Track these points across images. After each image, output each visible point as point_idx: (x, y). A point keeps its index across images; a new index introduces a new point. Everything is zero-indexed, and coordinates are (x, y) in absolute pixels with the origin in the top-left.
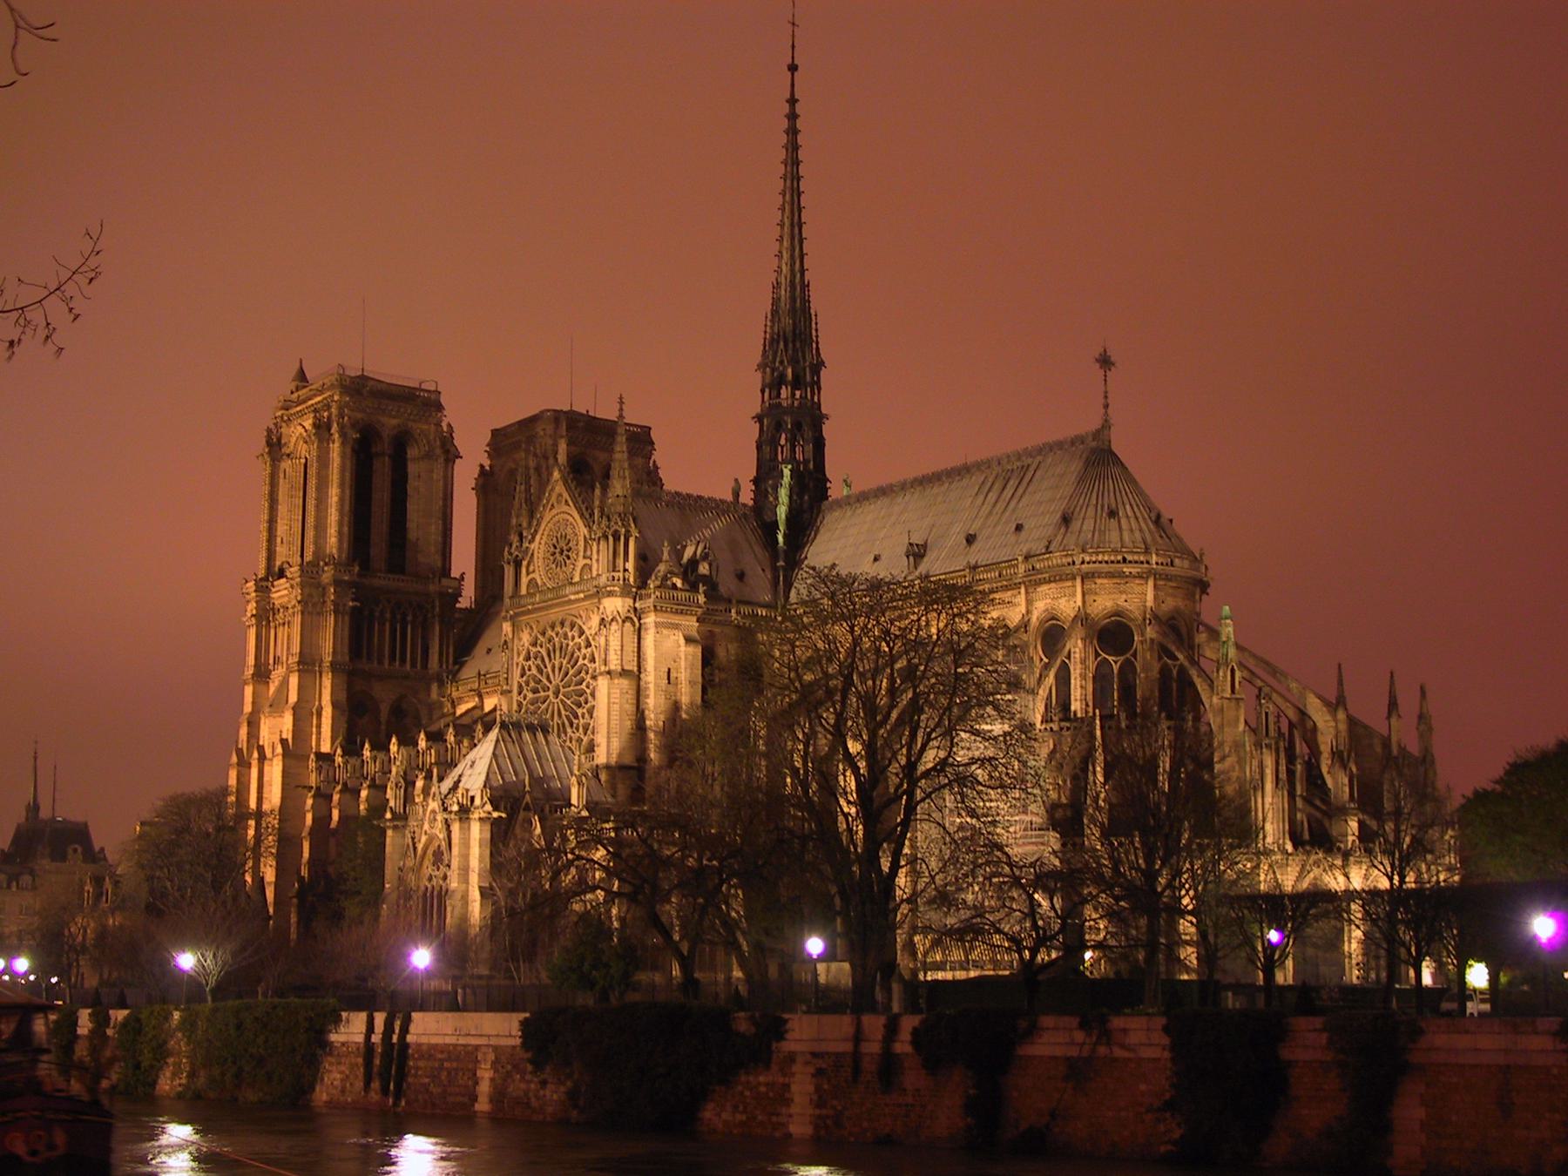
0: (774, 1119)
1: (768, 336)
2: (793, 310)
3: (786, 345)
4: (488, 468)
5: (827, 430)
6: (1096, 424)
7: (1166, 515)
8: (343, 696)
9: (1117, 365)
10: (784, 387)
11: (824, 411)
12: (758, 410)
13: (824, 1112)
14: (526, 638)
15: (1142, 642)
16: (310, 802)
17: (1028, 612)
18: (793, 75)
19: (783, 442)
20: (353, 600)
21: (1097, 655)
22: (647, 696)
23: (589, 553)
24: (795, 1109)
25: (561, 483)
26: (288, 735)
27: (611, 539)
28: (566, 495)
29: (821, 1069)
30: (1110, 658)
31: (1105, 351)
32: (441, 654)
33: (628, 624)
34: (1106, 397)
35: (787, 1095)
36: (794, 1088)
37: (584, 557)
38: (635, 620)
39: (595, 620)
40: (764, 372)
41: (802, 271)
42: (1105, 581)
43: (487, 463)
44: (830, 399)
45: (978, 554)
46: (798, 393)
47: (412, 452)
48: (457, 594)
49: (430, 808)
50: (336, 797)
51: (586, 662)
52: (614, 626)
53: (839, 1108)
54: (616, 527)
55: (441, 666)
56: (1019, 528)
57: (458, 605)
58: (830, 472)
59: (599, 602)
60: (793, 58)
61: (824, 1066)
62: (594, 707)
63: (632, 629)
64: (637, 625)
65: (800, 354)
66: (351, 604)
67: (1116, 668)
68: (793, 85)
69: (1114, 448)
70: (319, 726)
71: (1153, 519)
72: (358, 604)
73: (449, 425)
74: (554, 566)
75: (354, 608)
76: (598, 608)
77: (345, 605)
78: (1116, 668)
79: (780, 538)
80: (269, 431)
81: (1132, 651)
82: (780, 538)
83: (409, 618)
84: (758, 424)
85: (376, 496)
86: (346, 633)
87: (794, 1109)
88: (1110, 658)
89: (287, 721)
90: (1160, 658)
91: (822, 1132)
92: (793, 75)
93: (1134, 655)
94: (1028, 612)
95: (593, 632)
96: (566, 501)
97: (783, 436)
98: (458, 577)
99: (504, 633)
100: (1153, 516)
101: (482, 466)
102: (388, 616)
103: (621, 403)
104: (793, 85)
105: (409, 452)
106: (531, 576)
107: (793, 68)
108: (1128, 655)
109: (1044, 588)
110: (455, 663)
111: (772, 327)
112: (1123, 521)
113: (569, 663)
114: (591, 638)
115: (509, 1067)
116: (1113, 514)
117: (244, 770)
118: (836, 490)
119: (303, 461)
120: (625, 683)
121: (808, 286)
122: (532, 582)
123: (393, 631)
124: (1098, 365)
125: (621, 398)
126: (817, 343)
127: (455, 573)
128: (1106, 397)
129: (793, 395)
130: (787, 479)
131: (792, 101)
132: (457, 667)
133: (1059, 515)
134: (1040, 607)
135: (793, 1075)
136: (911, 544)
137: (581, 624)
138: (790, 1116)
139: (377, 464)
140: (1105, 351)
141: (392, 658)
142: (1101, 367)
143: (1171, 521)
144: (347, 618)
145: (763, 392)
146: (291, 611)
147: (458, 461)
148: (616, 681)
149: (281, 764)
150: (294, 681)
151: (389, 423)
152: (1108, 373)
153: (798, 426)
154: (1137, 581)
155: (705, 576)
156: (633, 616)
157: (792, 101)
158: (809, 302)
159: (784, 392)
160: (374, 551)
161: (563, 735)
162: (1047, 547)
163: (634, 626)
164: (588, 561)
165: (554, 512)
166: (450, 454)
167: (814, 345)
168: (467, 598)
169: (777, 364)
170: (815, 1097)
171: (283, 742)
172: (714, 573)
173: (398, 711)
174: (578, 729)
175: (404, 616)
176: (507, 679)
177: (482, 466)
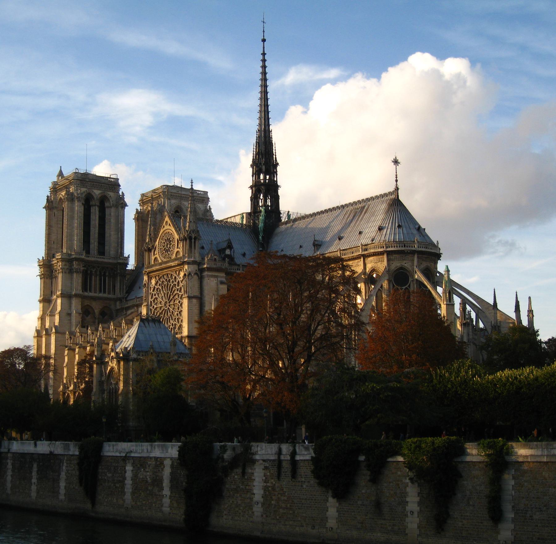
0: (247, 487)
1: (255, 153)
2: (265, 142)
3: (262, 157)
4: (139, 210)
5: (280, 192)
6: (392, 189)
7: (423, 226)
8: (80, 307)
9: (401, 163)
10: (262, 174)
11: (279, 184)
13: (268, 484)
14: (153, 282)
15: (413, 281)
16: (66, 352)
18: (264, 43)
19: (261, 197)
20: (83, 267)
21: (394, 286)
22: (205, 306)
23: (179, 246)
24: (255, 483)
25: (167, 217)
26: (57, 323)
27: (188, 241)
28: (169, 222)
29: (266, 466)
31: (396, 157)
32: (120, 289)
33: (196, 277)
34: (396, 177)
35: (253, 478)
36: (255, 474)
37: (177, 248)
38: (199, 274)
39: (182, 274)
40: (253, 168)
41: (269, 125)
42: (396, 255)
45: (344, 245)
46: (268, 177)
47: (107, 204)
48: (126, 264)
49: (111, 355)
50: (77, 350)
51: (178, 292)
52: (190, 277)
53: (274, 483)
54: (190, 235)
55: (120, 294)
56: (360, 233)
57: (127, 268)
59: (184, 267)
60: (264, 36)
61: (268, 465)
62: (182, 311)
63: (197, 278)
64: (200, 276)
65: (268, 160)
66: (82, 268)
68: (264, 48)
69: (401, 198)
70: (70, 320)
71: (417, 229)
72: (85, 268)
73: (122, 193)
74: (164, 252)
75: (83, 270)
76: (183, 269)
77: (80, 269)
79: (260, 238)
80: (48, 197)
81: (408, 285)
82: (260, 238)
83: (107, 274)
84: (251, 190)
85: (92, 223)
86: (80, 281)
87: (255, 484)
88: (399, 288)
89: (57, 318)
90: (420, 287)
91: (267, 493)
92: (264, 43)
93: (409, 286)
95: (181, 280)
96: (169, 224)
97: (262, 195)
98: (127, 256)
99: (145, 280)
100: (417, 227)
101: (137, 210)
102: (98, 273)
103: (192, 183)
104: (264, 48)
105: (106, 204)
106: (155, 256)
107: (264, 40)
108: (407, 286)
109: (371, 258)
110: (126, 293)
111: (256, 149)
112: (404, 229)
113: (171, 292)
114: (180, 282)
115: (139, 465)
117: (40, 338)
118: (284, 218)
119: (62, 209)
120: (194, 301)
121: (271, 131)
122: (156, 258)
123: (100, 280)
124: (393, 163)
125: (192, 181)
126: (275, 155)
127: (126, 255)
128: (396, 177)
129: (265, 178)
130: (263, 213)
131: (264, 54)
132: (127, 294)
133: (377, 227)
134: (369, 267)
135: (255, 469)
136: (315, 240)
137: (176, 276)
138: (254, 486)
139: (92, 210)
140: (396, 157)
141: (100, 291)
142: (394, 164)
143: (425, 229)
144: (81, 275)
145: (253, 176)
146: (58, 272)
147: (126, 208)
148: (191, 300)
149: (55, 336)
150: (59, 301)
151: (97, 193)
152: (397, 167)
154: (410, 255)
155: (228, 255)
156: (198, 272)
157: (264, 54)
158: (272, 138)
159: (262, 177)
160: (92, 246)
161: (169, 323)
162: (372, 240)
163: (199, 277)
164: (178, 250)
165: (164, 229)
166: (124, 205)
167: (274, 156)
168: (131, 265)
169: (259, 165)
170: (264, 478)
171: (56, 327)
172: (232, 254)
173: (103, 313)
174: (175, 320)
175: (105, 273)
176: (146, 299)
177: (137, 210)
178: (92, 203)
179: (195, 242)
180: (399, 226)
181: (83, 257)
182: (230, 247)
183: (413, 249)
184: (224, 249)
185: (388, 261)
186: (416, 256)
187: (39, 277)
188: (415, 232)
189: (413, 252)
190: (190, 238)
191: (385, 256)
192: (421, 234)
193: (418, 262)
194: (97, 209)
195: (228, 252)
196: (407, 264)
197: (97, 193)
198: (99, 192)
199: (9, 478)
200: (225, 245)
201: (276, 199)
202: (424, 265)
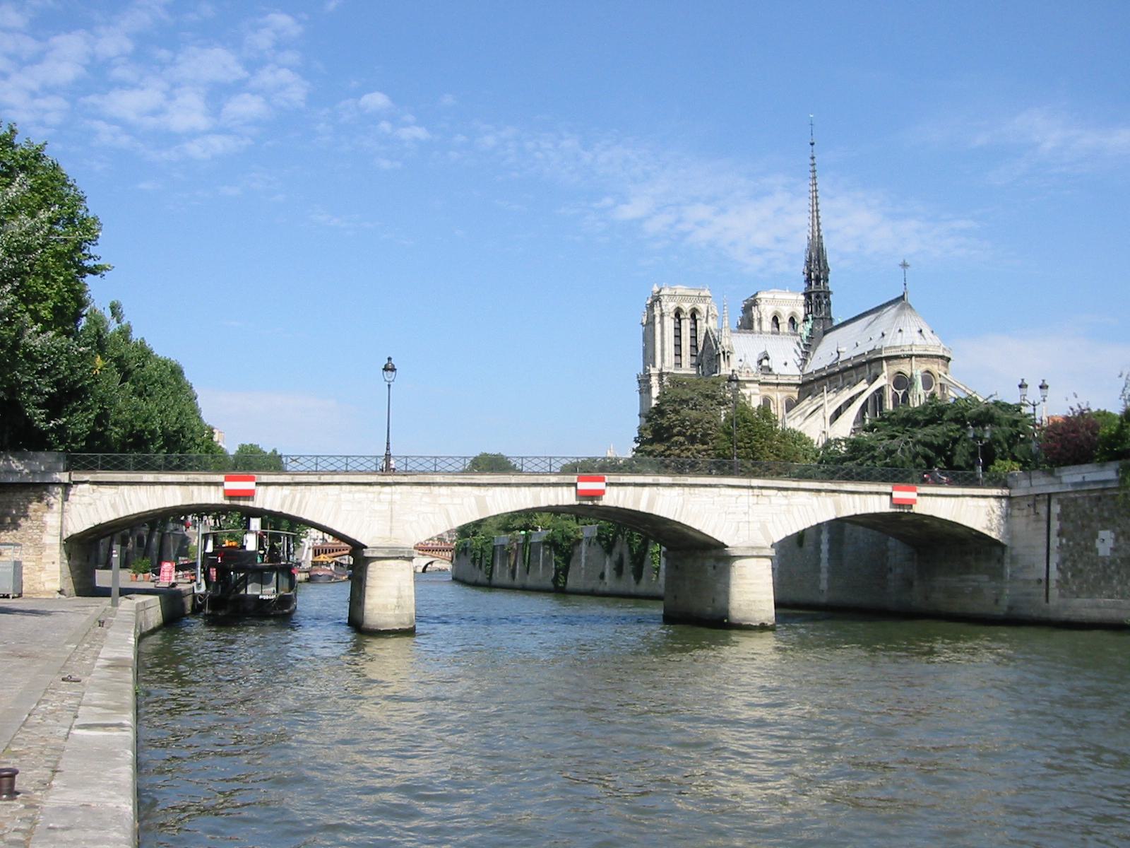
11: (830, 289)
12: (803, 291)
17: (870, 373)
30: (897, 391)
43: (741, 315)
44: (831, 285)
47: (697, 317)
58: (833, 316)
67: (900, 396)
78: (900, 396)
88: (897, 391)
94: (870, 373)
107: (812, 144)
109: (873, 364)
112: (904, 333)
116: (900, 331)
139: (683, 322)
151: (687, 307)
153: (818, 297)
157: (813, 158)
160: (683, 359)
178: (682, 316)
179: (728, 357)
180: (900, 331)
181: (671, 371)
182: (767, 358)
183: (910, 353)
184: (761, 361)
185: (888, 365)
186: (913, 358)
187: (638, 393)
188: (918, 335)
189: (910, 357)
190: (724, 353)
191: (884, 363)
192: (923, 336)
193: (916, 365)
194: (688, 322)
195: (765, 363)
196: (905, 367)
197: (687, 307)
198: (689, 304)
199: (498, 565)
200: (762, 357)
201: (829, 304)
202: (924, 367)
